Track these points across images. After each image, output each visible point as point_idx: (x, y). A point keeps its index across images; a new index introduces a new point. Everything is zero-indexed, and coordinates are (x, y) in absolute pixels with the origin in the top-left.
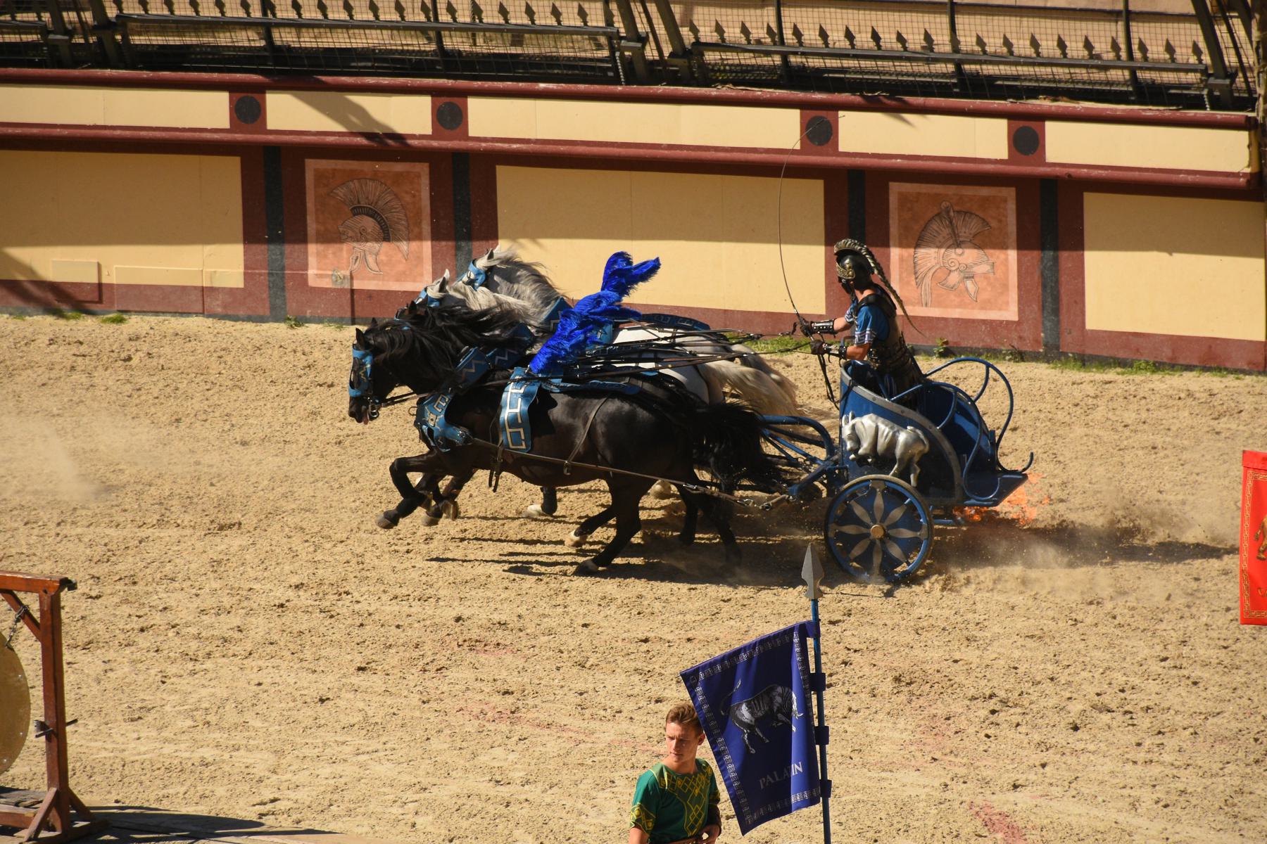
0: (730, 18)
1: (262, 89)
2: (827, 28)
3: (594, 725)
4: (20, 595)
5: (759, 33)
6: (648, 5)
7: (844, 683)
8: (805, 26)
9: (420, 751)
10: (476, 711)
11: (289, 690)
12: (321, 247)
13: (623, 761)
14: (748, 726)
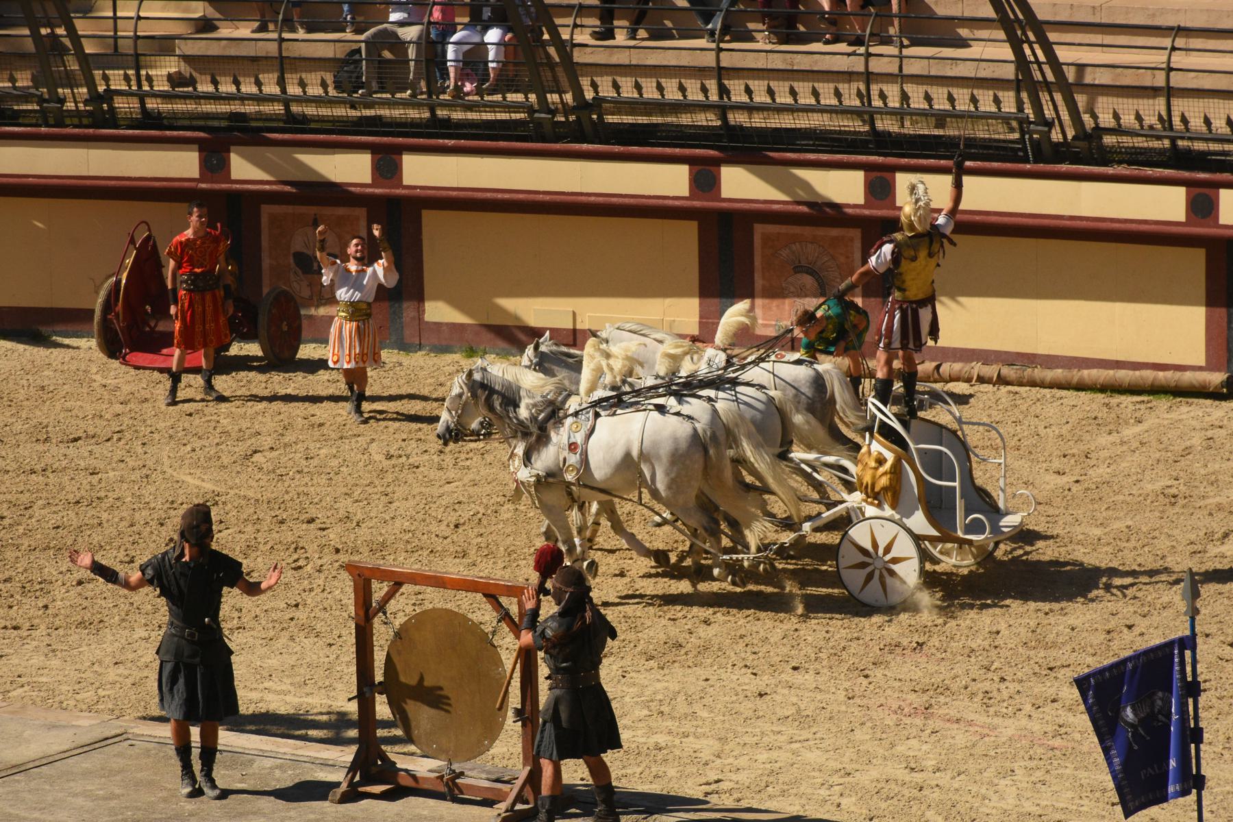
0: (1125, 106)
1: (718, 163)
2: (1211, 116)
3: (996, 721)
4: (504, 600)
5: (1151, 120)
6: (1054, 94)
7: (1216, 689)
8: (1192, 114)
9: (845, 741)
10: (895, 707)
11: (732, 685)
12: (767, 301)
13: (1022, 753)
14: (1132, 725)
